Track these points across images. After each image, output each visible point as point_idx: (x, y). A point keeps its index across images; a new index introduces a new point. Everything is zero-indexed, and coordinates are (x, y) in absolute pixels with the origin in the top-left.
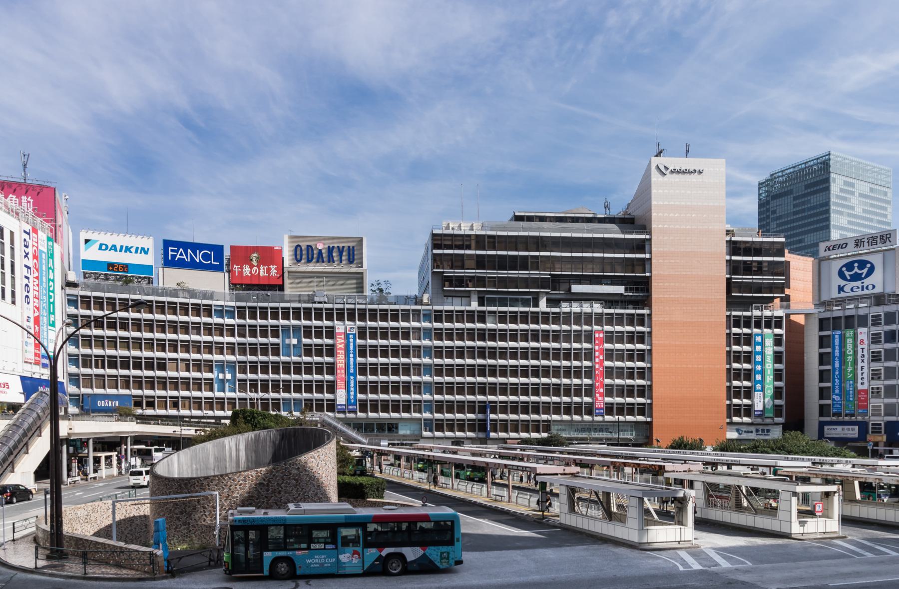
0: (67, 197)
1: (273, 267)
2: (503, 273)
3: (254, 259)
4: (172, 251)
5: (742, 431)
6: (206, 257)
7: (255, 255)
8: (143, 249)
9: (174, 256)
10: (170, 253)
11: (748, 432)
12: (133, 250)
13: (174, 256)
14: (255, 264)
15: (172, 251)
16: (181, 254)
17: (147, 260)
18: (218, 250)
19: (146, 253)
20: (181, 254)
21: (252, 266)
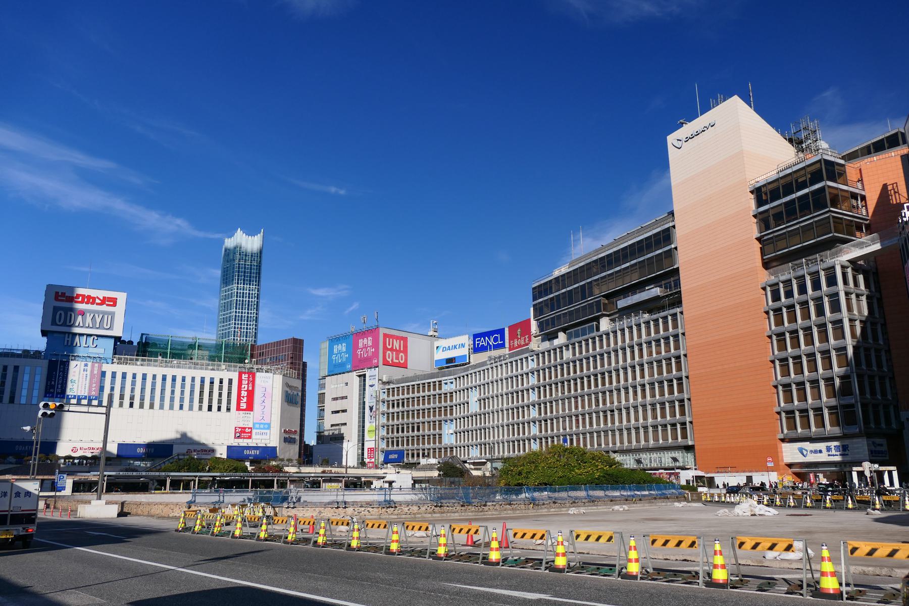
0: (435, 322)
1: (527, 336)
2: (573, 307)
3: (519, 333)
4: (478, 341)
5: (807, 451)
6: (496, 340)
7: (519, 330)
8: (462, 344)
9: (478, 344)
10: (477, 343)
11: (816, 452)
12: (457, 347)
13: (478, 344)
14: (519, 337)
15: (478, 341)
16: (482, 342)
17: (464, 351)
18: (501, 332)
19: (464, 347)
20: (482, 342)
21: (518, 339)
